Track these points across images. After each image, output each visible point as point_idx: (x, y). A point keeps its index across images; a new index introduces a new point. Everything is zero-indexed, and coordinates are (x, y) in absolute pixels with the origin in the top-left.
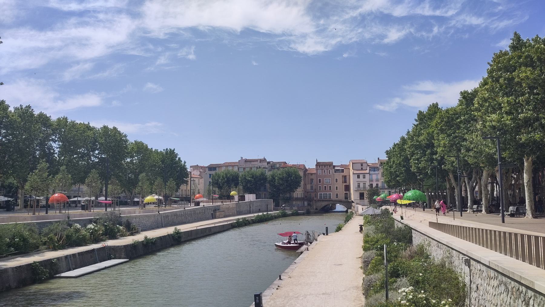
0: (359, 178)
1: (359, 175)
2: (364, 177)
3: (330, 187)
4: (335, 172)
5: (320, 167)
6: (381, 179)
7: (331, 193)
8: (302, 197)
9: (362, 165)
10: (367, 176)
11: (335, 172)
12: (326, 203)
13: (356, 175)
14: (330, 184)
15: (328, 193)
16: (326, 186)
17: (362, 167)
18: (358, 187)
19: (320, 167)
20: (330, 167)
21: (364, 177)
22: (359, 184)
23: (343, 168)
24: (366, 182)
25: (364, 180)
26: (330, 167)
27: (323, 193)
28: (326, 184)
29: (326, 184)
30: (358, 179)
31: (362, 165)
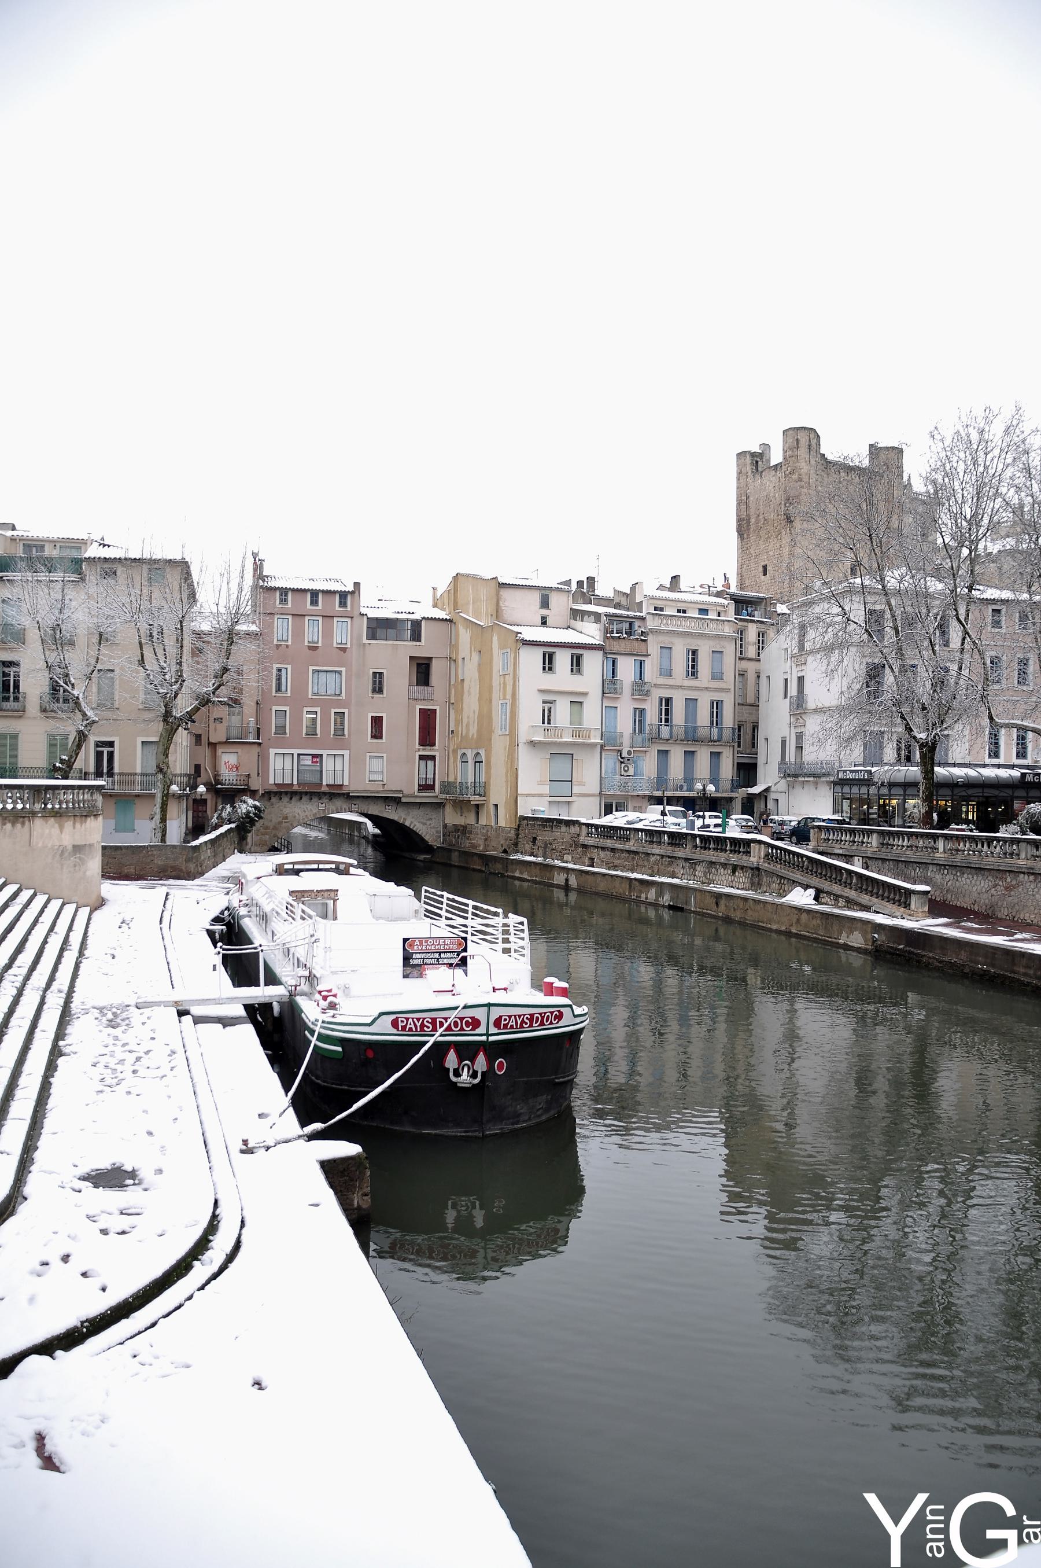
1: (551, 656)
2: (577, 663)
7: (346, 753)
9: (545, 604)
10: (593, 663)
11: (372, 635)
12: (309, 807)
15: (325, 753)
17: (545, 612)
21: (577, 663)
22: (547, 706)
24: (585, 694)
27: (296, 752)
28: (313, 702)
30: (548, 676)
31: (545, 604)
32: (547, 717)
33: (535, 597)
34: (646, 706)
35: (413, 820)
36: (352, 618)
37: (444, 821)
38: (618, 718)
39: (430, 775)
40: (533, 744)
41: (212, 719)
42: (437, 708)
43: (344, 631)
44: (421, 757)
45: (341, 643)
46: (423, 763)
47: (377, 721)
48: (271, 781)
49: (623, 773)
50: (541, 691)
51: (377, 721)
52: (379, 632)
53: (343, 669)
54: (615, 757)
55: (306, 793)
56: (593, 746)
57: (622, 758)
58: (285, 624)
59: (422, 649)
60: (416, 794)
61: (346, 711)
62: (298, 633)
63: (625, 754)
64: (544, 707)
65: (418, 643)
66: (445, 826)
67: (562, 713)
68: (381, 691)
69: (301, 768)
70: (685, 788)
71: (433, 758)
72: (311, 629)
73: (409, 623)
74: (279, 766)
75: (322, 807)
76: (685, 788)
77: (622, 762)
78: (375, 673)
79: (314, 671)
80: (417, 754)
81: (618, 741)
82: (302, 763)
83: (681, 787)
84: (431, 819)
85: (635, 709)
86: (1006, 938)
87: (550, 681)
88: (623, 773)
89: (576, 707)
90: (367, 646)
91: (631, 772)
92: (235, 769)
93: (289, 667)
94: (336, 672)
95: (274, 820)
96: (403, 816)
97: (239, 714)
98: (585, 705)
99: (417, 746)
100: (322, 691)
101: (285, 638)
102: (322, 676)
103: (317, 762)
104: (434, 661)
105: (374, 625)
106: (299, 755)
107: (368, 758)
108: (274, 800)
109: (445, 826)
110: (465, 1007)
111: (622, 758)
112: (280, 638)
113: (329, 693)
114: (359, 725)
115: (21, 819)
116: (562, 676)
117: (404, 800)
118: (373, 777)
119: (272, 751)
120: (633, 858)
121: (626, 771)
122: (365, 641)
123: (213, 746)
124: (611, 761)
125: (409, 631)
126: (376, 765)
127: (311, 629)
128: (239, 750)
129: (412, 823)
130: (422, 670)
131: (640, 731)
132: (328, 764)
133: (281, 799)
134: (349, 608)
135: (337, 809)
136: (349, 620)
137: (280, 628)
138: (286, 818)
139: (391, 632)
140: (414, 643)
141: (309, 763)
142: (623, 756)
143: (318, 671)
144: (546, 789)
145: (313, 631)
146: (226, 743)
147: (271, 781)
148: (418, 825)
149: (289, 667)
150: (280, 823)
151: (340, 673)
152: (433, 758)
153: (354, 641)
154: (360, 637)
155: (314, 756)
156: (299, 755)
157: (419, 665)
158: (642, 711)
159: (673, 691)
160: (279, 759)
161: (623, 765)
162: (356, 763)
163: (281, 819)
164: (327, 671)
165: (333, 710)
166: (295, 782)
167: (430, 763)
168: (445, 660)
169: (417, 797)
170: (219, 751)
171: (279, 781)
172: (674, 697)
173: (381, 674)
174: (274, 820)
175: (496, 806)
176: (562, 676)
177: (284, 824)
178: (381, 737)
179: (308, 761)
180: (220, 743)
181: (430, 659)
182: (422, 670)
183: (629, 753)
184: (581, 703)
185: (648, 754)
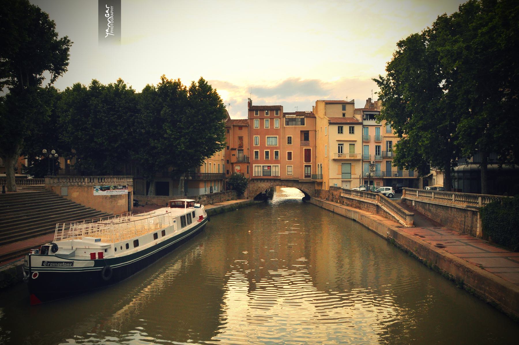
0: (342, 133)
2: (352, 131)
3: (277, 153)
4: (287, 124)
5: (257, 114)
6: (385, 137)
8: (221, 171)
10: (358, 129)
11: (287, 124)
12: (267, 184)
13: (335, 128)
14: (276, 148)
15: (272, 165)
16: (269, 150)
17: (344, 112)
18: (339, 152)
19: (257, 114)
20: (277, 114)
21: (352, 131)
22: (340, 146)
23: (303, 117)
24: (356, 141)
25: (352, 137)
26: (277, 114)
27: (262, 165)
28: (267, 148)
29: (267, 148)
30: (340, 135)
31: (344, 109)
32: (340, 149)
33: (340, 106)
34: (381, 145)
35: (304, 188)
36: (280, 118)
37: (315, 189)
38: (369, 149)
39: (309, 172)
40: (335, 160)
41: (231, 155)
42: (311, 148)
43: (268, 123)
44: (306, 166)
45: (277, 127)
46: (306, 168)
47: (290, 154)
48: (254, 175)
49: (371, 170)
50: (337, 141)
51: (290, 154)
52: (290, 123)
53: (278, 136)
54: (368, 164)
55: (266, 179)
56: (359, 160)
57: (371, 164)
58: (257, 122)
59: (305, 127)
60: (304, 179)
61: (279, 150)
62: (262, 124)
63: (372, 163)
64: (339, 147)
65: (303, 126)
66: (315, 190)
67: (346, 148)
68: (291, 143)
69: (264, 170)
70: (398, 175)
71: (310, 166)
72: (266, 123)
73: (300, 119)
74: (256, 170)
75: (272, 184)
76: (398, 175)
77: (371, 166)
78: (288, 137)
79: (268, 137)
80: (304, 165)
81: (369, 158)
82: (264, 169)
83: (396, 175)
84: (311, 188)
85: (376, 146)
86: (90, 218)
87: (341, 137)
88: (371, 170)
89: (352, 146)
90: (286, 128)
91: (374, 169)
92: (239, 171)
93: (259, 136)
94: (275, 137)
95: (255, 188)
96: (301, 187)
97: (242, 153)
98: (355, 145)
99: (304, 162)
100: (271, 144)
101: (257, 126)
102: (271, 139)
103: (269, 168)
104: (310, 131)
105: (288, 120)
106: (263, 166)
107: (287, 167)
108: (255, 182)
109: (315, 190)
110: (67, 238)
111: (371, 164)
112: (256, 127)
113: (273, 144)
114: (283, 155)
115: (90, 187)
116: (346, 135)
117: (300, 181)
118: (289, 173)
119: (254, 165)
120: (352, 201)
121: (372, 169)
122: (285, 126)
123: (232, 164)
124: (366, 166)
125: (300, 122)
126: (290, 169)
127: (266, 123)
128: (241, 165)
129: (304, 189)
130: (305, 135)
131: (379, 154)
132: (273, 169)
133: (257, 181)
134: (279, 115)
135: (277, 184)
136: (279, 119)
137: (256, 123)
138: (260, 188)
139: (294, 122)
140: (302, 126)
141: (267, 169)
142: (371, 163)
143: (269, 137)
144: (340, 176)
145: (267, 124)
146: (236, 163)
147: (254, 175)
148: (306, 190)
149: (259, 136)
150: (257, 189)
151: (276, 137)
152: (310, 166)
153: (281, 127)
154: (283, 125)
155: (268, 166)
156: (263, 166)
157: (305, 134)
158: (379, 147)
159: (392, 138)
160: (256, 168)
161: (371, 167)
162: (283, 169)
163: (257, 188)
164: (272, 137)
165: (274, 151)
166: (262, 176)
167: (309, 168)
168: (313, 131)
169: (304, 180)
170: (234, 165)
171: (257, 175)
172: (393, 141)
173: (291, 137)
174: (255, 188)
175: (325, 182)
176: (346, 135)
177: (259, 190)
178: (291, 159)
179: (266, 168)
180: (234, 163)
181: (308, 131)
182: (305, 135)
183: (373, 162)
184: (354, 144)
185: (382, 163)
